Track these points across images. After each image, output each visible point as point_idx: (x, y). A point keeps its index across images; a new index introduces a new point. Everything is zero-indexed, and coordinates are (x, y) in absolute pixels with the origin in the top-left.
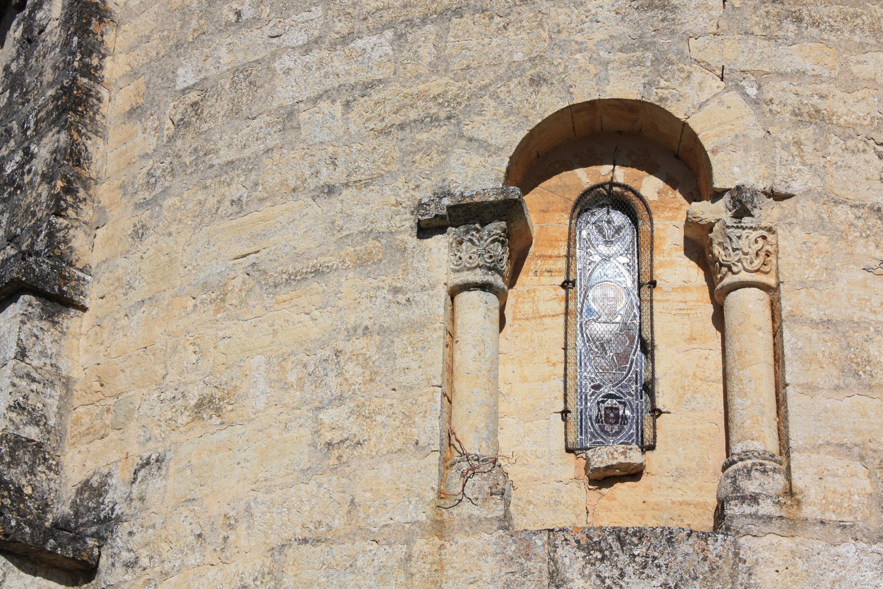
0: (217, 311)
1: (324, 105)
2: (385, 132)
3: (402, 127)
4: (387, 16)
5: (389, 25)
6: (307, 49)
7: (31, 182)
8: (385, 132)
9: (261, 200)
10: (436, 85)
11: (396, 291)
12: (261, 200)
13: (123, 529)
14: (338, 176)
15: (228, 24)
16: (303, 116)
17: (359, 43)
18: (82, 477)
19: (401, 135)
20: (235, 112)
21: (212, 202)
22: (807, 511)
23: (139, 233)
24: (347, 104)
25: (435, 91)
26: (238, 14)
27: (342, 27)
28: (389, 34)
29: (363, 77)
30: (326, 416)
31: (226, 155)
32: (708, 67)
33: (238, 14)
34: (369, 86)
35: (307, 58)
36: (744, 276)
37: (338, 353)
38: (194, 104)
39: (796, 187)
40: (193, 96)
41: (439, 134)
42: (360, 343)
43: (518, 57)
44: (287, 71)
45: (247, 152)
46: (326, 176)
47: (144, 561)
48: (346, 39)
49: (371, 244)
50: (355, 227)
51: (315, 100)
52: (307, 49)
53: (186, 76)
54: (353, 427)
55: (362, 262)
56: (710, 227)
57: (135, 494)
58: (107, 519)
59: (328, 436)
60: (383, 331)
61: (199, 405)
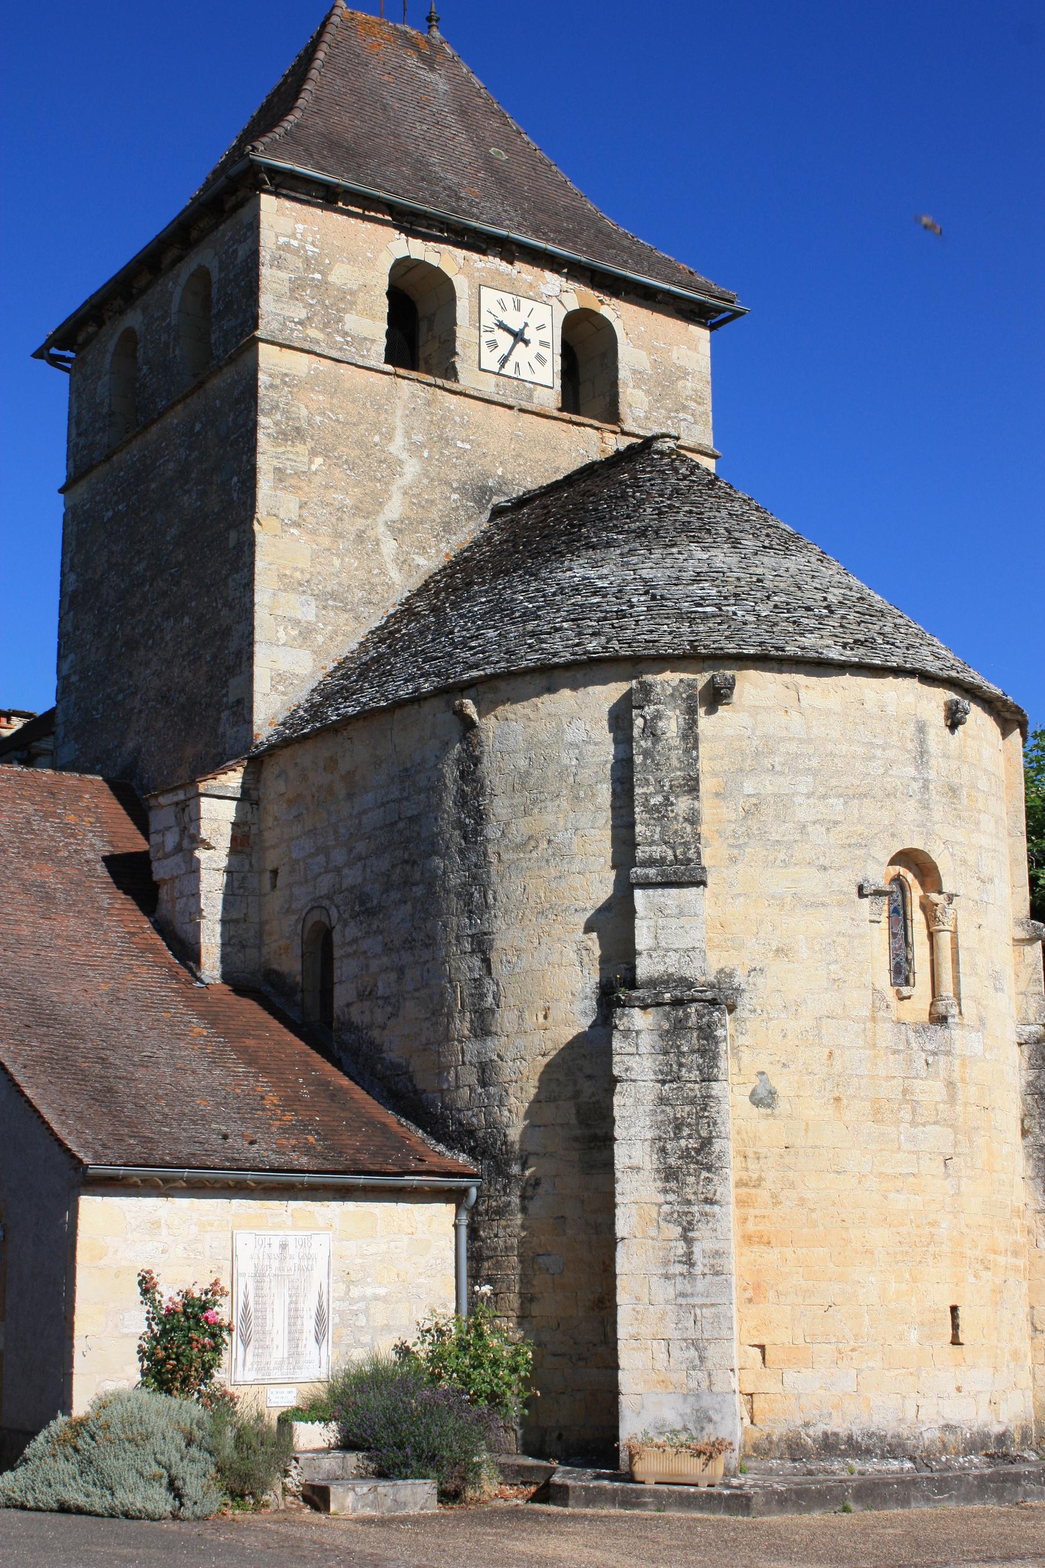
0: (780, 910)
1: (818, 826)
2: (843, 847)
3: (849, 846)
4: (840, 790)
5: (841, 796)
6: (809, 796)
7: (675, 818)
8: (843, 847)
9: (796, 864)
10: (860, 829)
11: (853, 919)
12: (796, 864)
13: (746, 995)
14: (826, 863)
15: (768, 769)
16: (810, 829)
17: (830, 801)
18: (720, 966)
19: (851, 849)
20: (777, 817)
21: (771, 858)
22: (965, 1021)
23: (734, 860)
24: (828, 829)
25: (859, 832)
26: (773, 766)
27: (822, 790)
28: (842, 800)
29: (833, 818)
30: (832, 967)
31: (775, 837)
32: (940, 838)
33: (773, 766)
34: (836, 823)
35: (809, 801)
36: (947, 927)
37: (834, 942)
38: (755, 805)
39: (961, 893)
40: (754, 800)
41: (862, 852)
42: (841, 939)
43: (886, 822)
44: (800, 805)
45: (785, 839)
46: (822, 861)
47: (759, 1011)
48: (825, 797)
49: (842, 897)
50: (835, 888)
51: (814, 823)
52: (809, 796)
53: (749, 788)
54: (841, 974)
55: (840, 904)
56: (937, 905)
57: (751, 981)
58: (737, 989)
59: (833, 976)
60: (849, 936)
61: (777, 950)
